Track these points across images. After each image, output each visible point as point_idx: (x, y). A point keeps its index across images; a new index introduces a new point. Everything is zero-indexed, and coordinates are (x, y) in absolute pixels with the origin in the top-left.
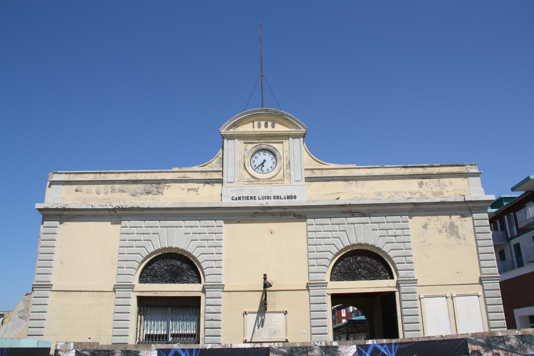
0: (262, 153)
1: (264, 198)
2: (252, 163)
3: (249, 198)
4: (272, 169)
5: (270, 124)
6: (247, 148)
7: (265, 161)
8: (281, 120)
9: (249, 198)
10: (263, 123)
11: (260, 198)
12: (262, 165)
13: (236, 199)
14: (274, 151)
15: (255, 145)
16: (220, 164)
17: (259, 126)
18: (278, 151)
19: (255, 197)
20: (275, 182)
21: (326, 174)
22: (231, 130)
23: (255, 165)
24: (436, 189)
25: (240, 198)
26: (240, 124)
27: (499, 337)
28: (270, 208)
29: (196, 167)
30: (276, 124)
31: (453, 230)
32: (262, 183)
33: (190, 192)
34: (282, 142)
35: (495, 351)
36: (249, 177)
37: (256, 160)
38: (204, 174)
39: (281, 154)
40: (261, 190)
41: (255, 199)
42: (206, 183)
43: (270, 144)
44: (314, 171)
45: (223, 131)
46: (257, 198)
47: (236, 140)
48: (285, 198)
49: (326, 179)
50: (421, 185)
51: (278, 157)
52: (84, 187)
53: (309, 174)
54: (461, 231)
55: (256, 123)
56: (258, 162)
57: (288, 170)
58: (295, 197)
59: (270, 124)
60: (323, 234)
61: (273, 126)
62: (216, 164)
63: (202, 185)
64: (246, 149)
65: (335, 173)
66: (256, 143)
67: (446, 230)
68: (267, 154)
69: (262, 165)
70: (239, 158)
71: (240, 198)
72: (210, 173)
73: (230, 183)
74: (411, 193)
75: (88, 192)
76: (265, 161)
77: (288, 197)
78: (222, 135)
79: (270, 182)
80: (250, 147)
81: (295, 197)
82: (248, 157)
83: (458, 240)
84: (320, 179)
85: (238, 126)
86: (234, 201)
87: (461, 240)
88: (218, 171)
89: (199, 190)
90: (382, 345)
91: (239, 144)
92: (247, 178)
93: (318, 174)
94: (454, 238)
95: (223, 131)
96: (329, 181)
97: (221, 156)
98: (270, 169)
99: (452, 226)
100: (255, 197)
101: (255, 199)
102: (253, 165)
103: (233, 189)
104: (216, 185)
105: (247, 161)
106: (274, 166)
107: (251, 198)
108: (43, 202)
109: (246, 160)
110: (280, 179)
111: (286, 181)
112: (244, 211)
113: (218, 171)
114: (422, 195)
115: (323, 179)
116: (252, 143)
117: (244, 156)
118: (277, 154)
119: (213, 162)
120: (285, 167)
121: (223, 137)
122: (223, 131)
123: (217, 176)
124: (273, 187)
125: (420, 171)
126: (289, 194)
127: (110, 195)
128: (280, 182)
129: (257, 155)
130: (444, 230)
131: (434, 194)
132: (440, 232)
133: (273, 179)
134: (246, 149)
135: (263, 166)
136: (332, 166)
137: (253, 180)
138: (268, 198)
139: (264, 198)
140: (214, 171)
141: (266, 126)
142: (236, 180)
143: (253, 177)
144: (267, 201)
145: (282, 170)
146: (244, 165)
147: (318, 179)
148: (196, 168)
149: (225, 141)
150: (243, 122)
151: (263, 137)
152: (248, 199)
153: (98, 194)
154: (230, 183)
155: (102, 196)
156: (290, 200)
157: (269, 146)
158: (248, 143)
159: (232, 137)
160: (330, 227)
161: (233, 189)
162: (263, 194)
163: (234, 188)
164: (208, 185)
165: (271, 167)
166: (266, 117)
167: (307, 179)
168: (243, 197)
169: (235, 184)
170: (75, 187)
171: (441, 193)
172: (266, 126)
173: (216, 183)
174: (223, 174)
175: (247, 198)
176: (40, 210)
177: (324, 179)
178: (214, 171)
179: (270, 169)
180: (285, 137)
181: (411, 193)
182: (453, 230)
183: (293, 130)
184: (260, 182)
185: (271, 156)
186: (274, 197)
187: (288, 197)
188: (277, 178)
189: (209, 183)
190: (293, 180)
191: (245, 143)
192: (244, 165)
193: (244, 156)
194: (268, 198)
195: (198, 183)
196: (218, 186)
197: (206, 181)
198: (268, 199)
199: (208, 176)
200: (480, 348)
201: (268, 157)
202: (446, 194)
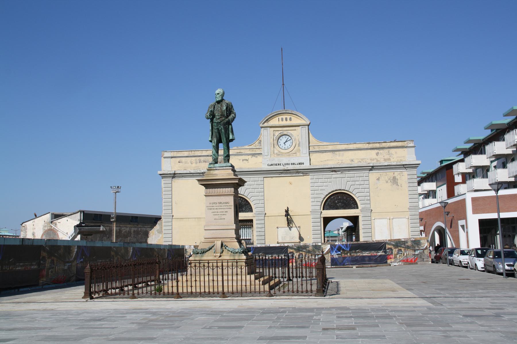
15: (280, 132)
17: (282, 120)
24: (387, 157)
25: (272, 165)
27: (403, 241)
31: (394, 180)
33: (244, 161)
35: (400, 248)
45: (261, 125)
50: (377, 154)
52: (183, 159)
54: (399, 182)
60: (319, 184)
67: (391, 181)
71: (272, 165)
74: (371, 160)
75: (186, 163)
77: (299, 164)
81: (303, 164)
83: (397, 187)
87: (400, 187)
90: (343, 245)
94: (395, 186)
99: (394, 178)
102: (279, 144)
105: (276, 142)
108: (161, 170)
114: (377, 161)
121: (262, 127)
123: (258, 151)
125: (378, 145)
126: (300, 162)
127: (198, 164)
130: (389, 181)
131: (385, 160)
132: (387, 182)
136: (325, 143)
138: (288, 164)
139: (286, 164)
144: (287, 166)
148: (247, 147)
153: (192, 164)
155: (194, 165)
160: (323, 180)
162: (286, 161)
169: (269, 157)
170: (178, 159)
171: (389, 159)
175: (276, 165)
176: (161, 175)
181: (371, 160)
182: (394, 180)
187: (299, 164)
188: (293, 152)
194: (288, 164)
200: (392, 247)
202: (392, 160)
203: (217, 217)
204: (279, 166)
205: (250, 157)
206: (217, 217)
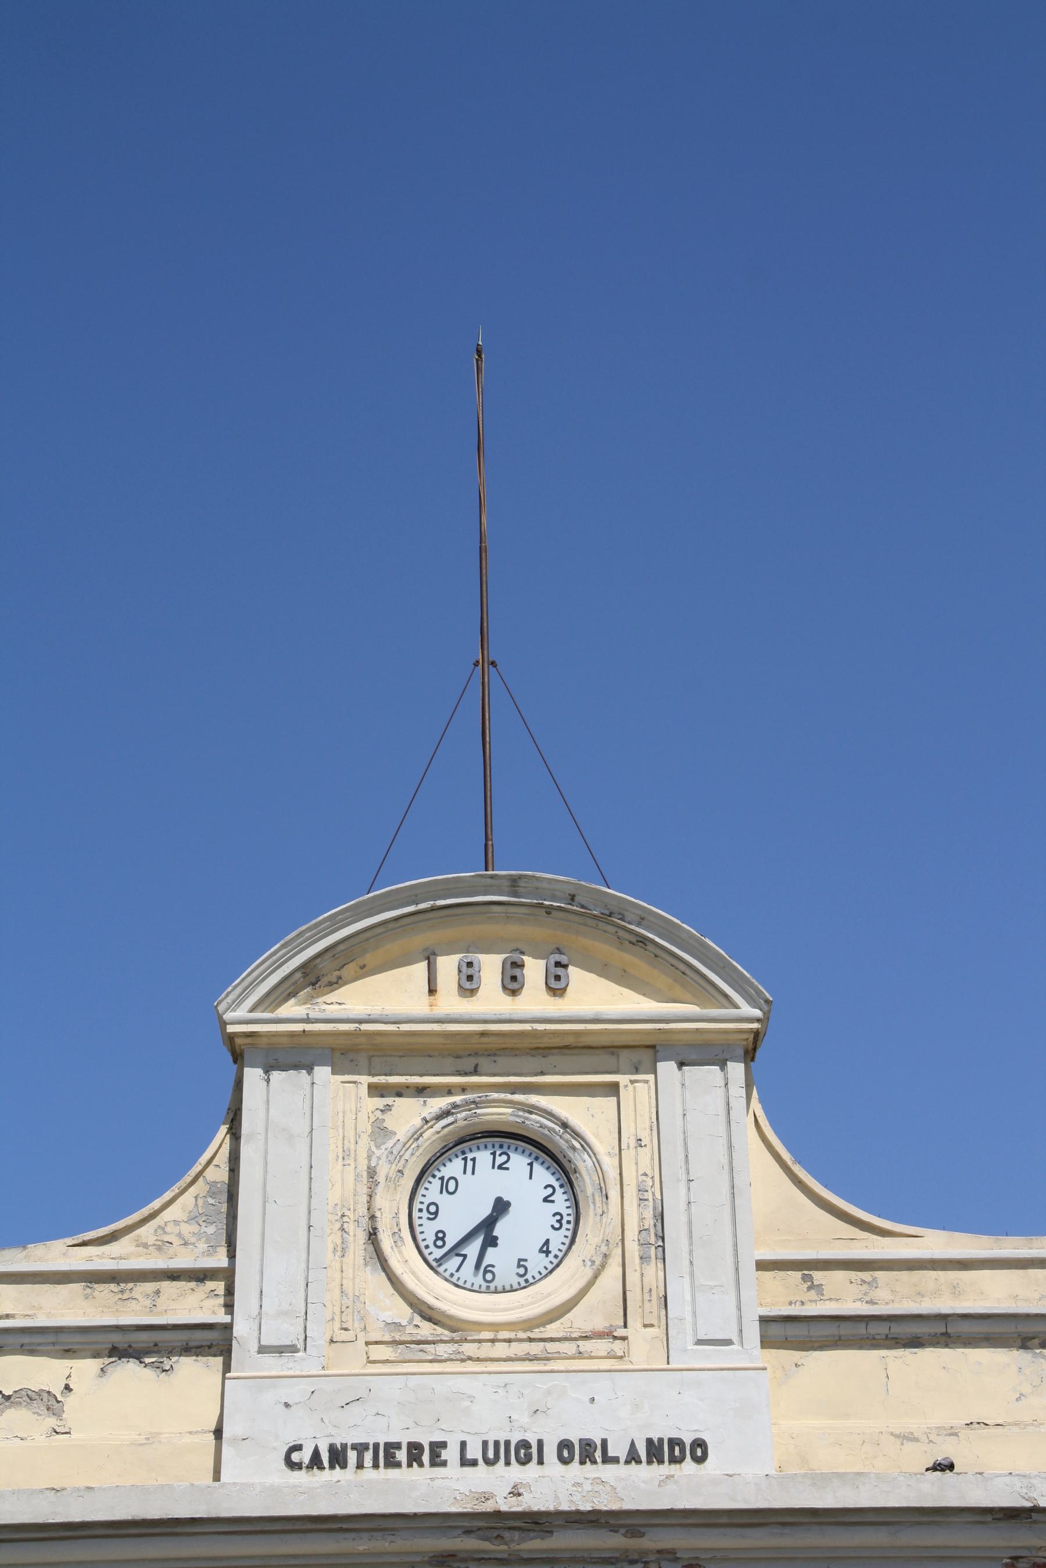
0: (483, 1157)
1: (499, 1453)
2: (421, 1220)
3: (402, 1456)
4: (545, 1261)
5: (534, 970)
6: (390, 1121)
7: (501, 1207)
8: (604, 949)
10: (491, 967)
11: (474, 1452)
12: (486, 1231)
13: (316, 1461)
14: (561, 1141)
16: (216, 1230)
18: (586, 1145)
19: (437, 1447)
20: (569, 1348)
21: (895, 1295)
22: (291, 1009)
25: (338, 1457)
26: (350, 969)
28: (536, 1522)
29: (59, 1246)
30: (570, 968)
32: (486, 1351)
34: (613, 1089)
36: (402, 1312)
37: (443, 1200)
38: (105, 1291)
39: (609, 1164)
40: (481, 1402)
41: (437, 1461)
42: (118, 1352)
43: (534, 1099)
44: (818, 1276)
45: (239, 1014)
46: (451, 1454)
47: (322, 1072)
48: (633, 1457)
49: (897, 1329)
51: (587, 1183)
53: (784, 1296)
55: (448, 965)
56: (460, 1215)
57: (652, 1271)
58: (699, 1451)
59: (534, 970)
61: (556, 986)
62: (187, 1229)
63: (89, 1366)
64: (380, 1132)
65: (955, 1290)
66: (449, 1090)
68: (519, 1162)
69: (486, 1231)
70: (340, 1185)
71: (338, 1457)
72: (150, 1287)
73: (280, 1350)
76: (501, 1207)
77: (655, 1451)
78: (231, 1038)
79: (536, 1348)
80: (408, 1115)
82: (393, 1182)
84: (861, 1329)
85: (336, 983)
86: (300, 1477)
88: (200, 1276)
89: (70, 1402)
91: (340, 1096)
92: (388, 1316)
93: (843, 1296)
95: (242, 1013)
96: (915, 1343)
97: (219, 1174)
98: (537, 1263)
100: (437, 1447)
101: (437, 1461)
102: (428, 1230)
103: (295, 1391)
104: (187, 1366)
105: (391, 1205)
106: (557, 1240)
107: (415, 1451)
109: (380, 1201)
110: (599, 1324)
111: (642, 1342)
112: (362, 1545)
113: (200, 1276)
115: (875, 1329)
116: (421, 1091)
117: (372, 1173)
118: (583, 1163)
119: (167, 1215)
120: (633, 1248)
121: (239, 1051)
122: (242, 1013)
124: (559, 1380)
126: (663, 1431)
128: (601, 1346)
129: (453, 1168)
133: (553, 1330)
134: (380, 1132)
135: (491, 1241)
137: (426, 1330)
138: (525, 1453)
139: (499, 1453)
140: (173, 1275)
141: (512, 983)
142: (318, 1333)
143: (426, 1313)
144: (516, 1473)
145: (614, 1269)
146: (373, 1236)
147: (846, 1330)
148: (57, 1255)
149: (253, 1076)
150: (369, 959)
151: (492, 1054)
152: (392, 1463)
154: (280, 1350)
156: (666, 1469)
157: (532, 1109)
158: (399, 1092)
159: (294, 1054)
161: (295, 1391)
163: (307, 1385)
164: (131, 1366)
166: (514, 929)
167: (775, 1330)
168: (361, 1448)
172: (512, 983)
173: (187, 1350)
174: (230, 1292)
175: (387, 1455)
177: (882, 1329)
178: (173, 1275)
179: (537, 1263)
180: (635, 1056)
183: (681, 1012)
184: (469, 1349)
185: (544, 1176)
186: (565, 1445)
187: (655, 1451)
188: (579, 1320)
189: (136, 1354)
190: (683, 1338)
191: (376, 1090)
192: (373, 1236)
193: (372, 1173)
194: (525, 1453)
195: (68, 1353)
196: (195, 1373)
197: (116, 1338)
198: (524, 1462)
199: (135, 1309)
201: (523, 1181)
204: (421, 1476)
205: (84, 1369)
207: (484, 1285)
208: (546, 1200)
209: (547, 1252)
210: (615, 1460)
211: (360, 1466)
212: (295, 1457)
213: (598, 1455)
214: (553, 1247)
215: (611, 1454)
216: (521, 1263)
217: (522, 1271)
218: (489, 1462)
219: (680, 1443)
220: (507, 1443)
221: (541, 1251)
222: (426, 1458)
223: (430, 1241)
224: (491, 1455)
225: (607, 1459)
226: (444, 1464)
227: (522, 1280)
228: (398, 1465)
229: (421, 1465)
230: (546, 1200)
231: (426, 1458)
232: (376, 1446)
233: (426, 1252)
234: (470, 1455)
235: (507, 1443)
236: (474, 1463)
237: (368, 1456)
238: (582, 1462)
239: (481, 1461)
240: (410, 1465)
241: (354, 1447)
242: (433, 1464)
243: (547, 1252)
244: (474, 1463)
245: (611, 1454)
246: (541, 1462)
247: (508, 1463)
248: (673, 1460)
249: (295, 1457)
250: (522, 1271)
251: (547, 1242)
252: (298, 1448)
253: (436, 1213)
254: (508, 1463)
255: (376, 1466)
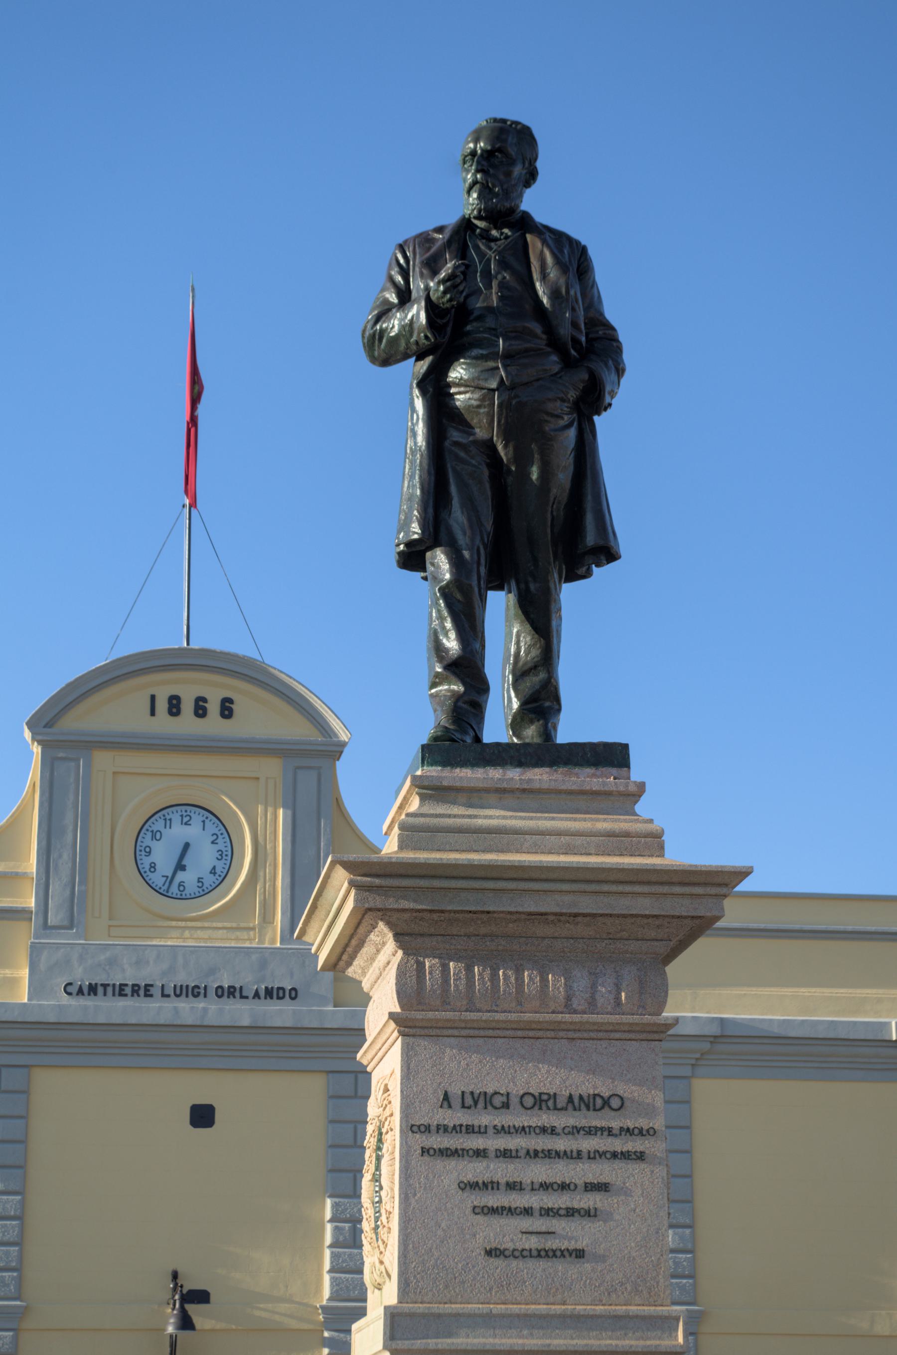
3: (128, 990)
9: (128, 990)
23: (153, 866)
25: (93, 989)
41: (148, 995)
46: (156, 991)
48: (257, 995)
71: (93, 989)
77: (269, 993)
98: (209, 880)
100: (148, 987)
107: (135, 989)
152: (122, 994)
165: (213, 871)
168: (105, 986)
179: (209, 880)
187: (269, 993)
194: (195, 992)
203: (508, 1232)
206: (508, 1232)
207: (179, 893)
208: (213, 842)
209: (215, 873)
210: (247, 997)
211: (105, 994)
212: (69, 989)
213: (237, 994)
214: (218, 871)
215: (244, 994)
216: (200, 880)
217: (200, 884)
218: (177, 996)
219: (283, 989)
220: (187, 986)
221: (211, 873)
222: (142, 992)
223: (147, 869)
224: (178, 992)
225: (242, 997)
226: (151, 996)
227: (200, 890)
228: (126, 995)
229: (139, 995)
230: (213, 842)
231: (142, 992)
232: (114, 985)
233: (145, 875)
234: (166, 992)
235: (187, 986)
236: (168, 996)
237: (110, 990)
238: (228, 997)
239: (172, 994)
240: (132, 995)
241: (102, 985)
242: (146, 995)
243: (215, 873)
244: (168, 996)
245: (244, 994)
246: (205, 996)
247: (187, 996)
248: (279, 998)
249: (69, 989)
250: (200, 884)
251: (214, 868)
252: (70, 984)
253: (150, 852)
254: (187, 996)
255: (114, 995)
